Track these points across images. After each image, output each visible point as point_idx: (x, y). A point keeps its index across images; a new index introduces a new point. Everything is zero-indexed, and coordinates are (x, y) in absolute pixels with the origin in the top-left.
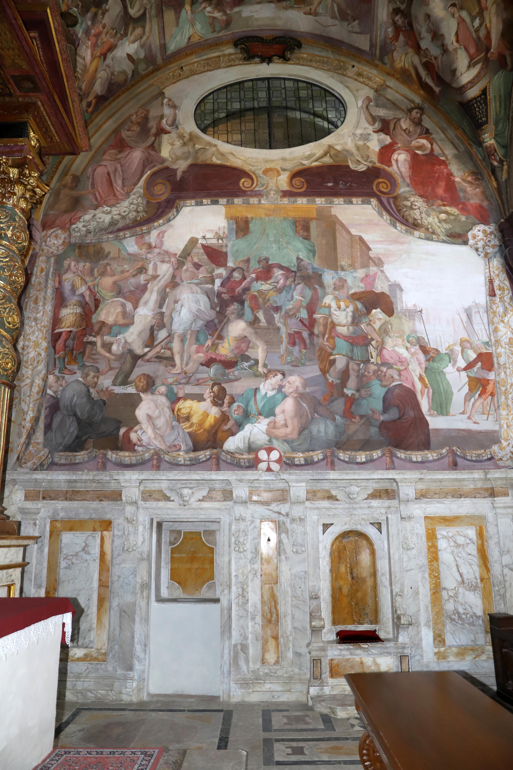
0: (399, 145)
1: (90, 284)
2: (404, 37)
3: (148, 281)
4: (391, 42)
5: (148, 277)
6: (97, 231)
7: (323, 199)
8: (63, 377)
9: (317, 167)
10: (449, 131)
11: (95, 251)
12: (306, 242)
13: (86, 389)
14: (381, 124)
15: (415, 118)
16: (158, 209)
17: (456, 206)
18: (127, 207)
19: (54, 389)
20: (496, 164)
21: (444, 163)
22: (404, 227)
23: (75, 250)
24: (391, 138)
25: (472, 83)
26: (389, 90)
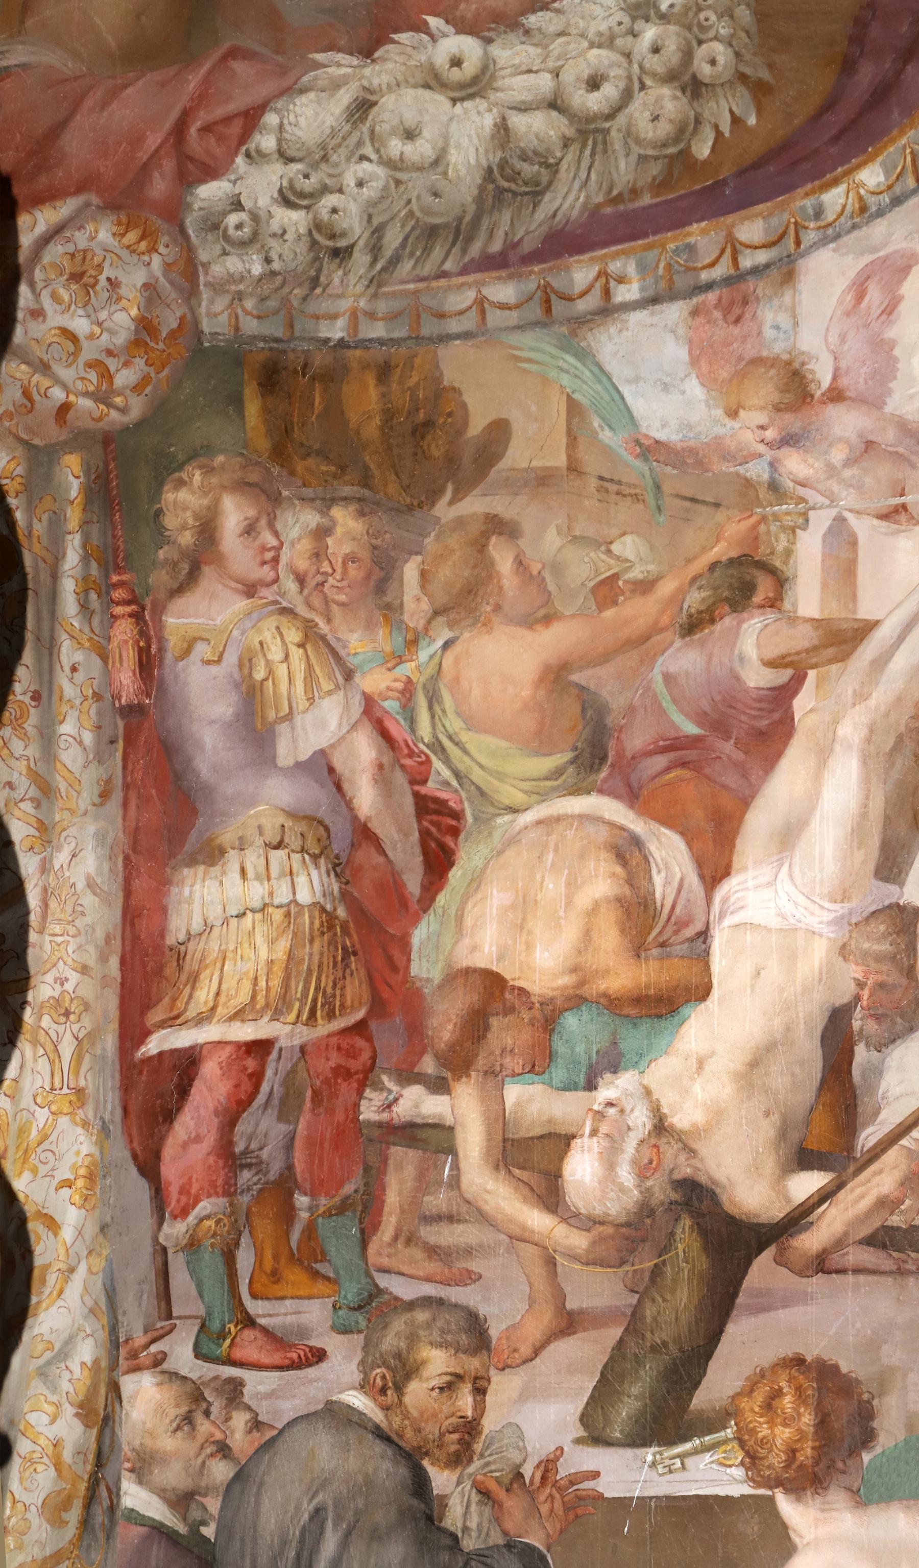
1: (375, 681)
3: (794, 671)
5: (801, 638)
6: (393, 239)
8: (234, 1389)
11: (389, 415)
13: (403, 1471)
16: (848, 66)
18: (607, 41)
19: (173, 1476)
23: (237, 402)
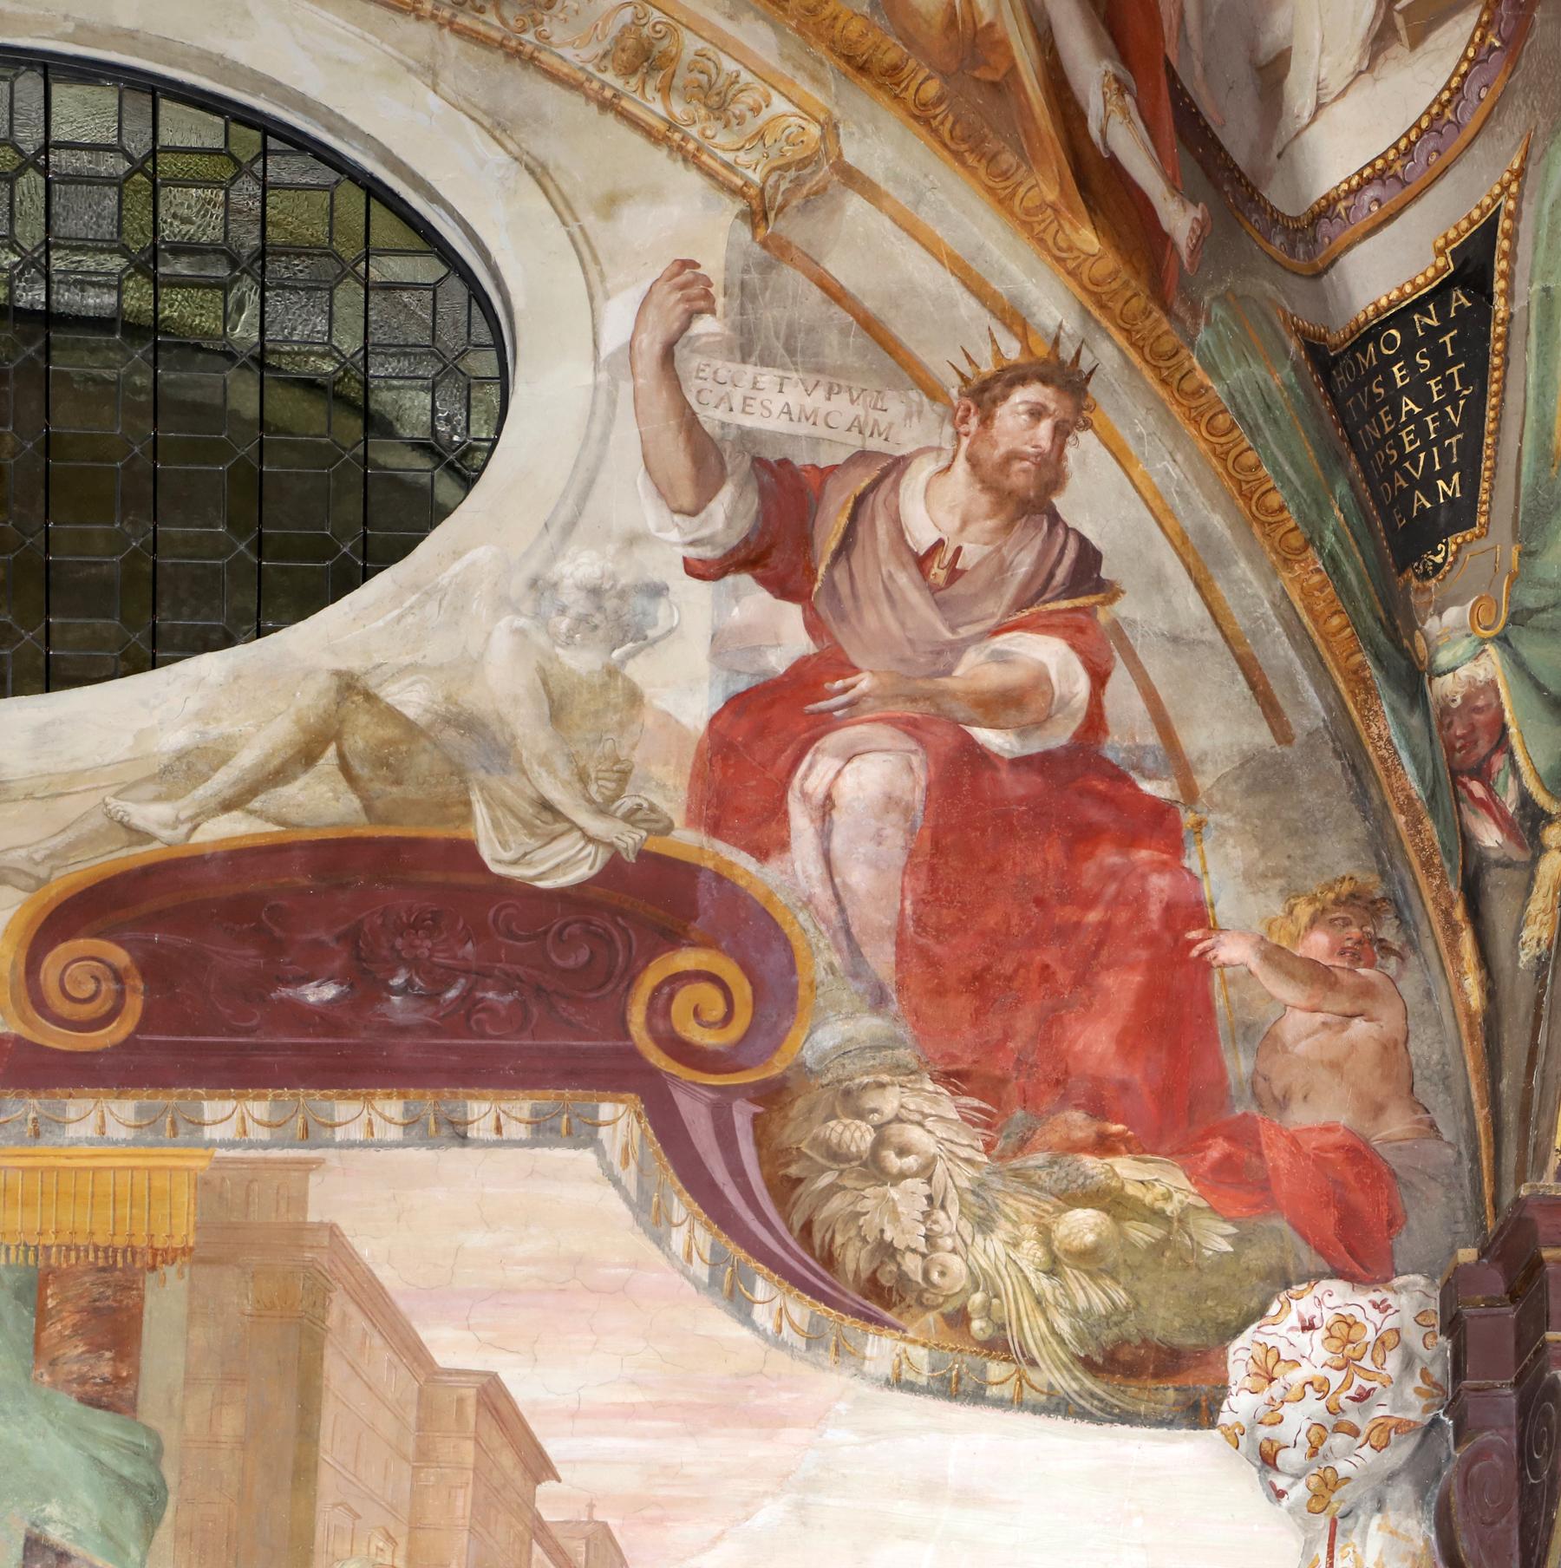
7: (258, 1108)
9: (240, 857)
10: (1243, 568)
12: (103, 1423)
14: (753, 502)
15: (1012, 456)
17: (1184, 1151)
21: (1160, 826)
22: (801, 1310)
24: (814, 626)
26: (855, 204)
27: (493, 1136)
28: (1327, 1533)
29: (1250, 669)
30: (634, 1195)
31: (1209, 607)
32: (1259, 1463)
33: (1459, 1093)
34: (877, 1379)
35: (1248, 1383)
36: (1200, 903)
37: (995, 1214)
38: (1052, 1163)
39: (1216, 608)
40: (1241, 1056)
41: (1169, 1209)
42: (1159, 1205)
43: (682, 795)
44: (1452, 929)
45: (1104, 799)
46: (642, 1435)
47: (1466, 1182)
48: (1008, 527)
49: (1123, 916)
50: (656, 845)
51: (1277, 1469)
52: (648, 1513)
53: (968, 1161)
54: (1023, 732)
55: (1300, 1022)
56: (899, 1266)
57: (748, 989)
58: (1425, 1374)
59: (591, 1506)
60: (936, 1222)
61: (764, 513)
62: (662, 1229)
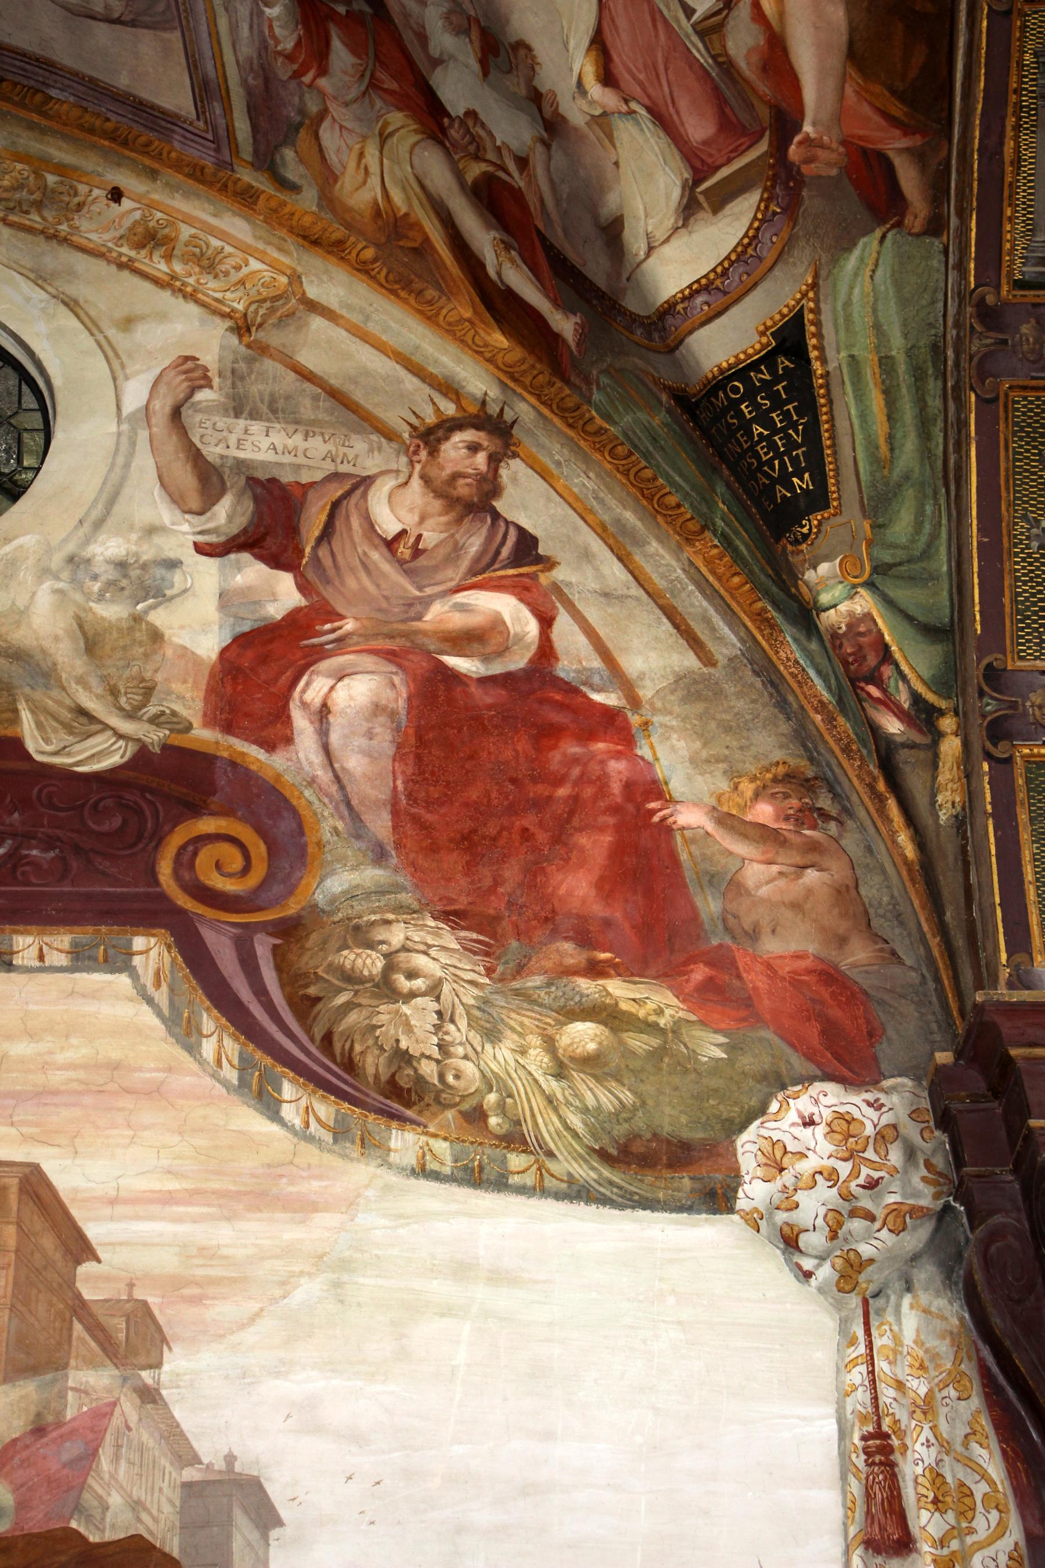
0: (349, 625)
2: (355, 52)
4: (297, 75)
10: (654, 546)
14: (249, 506)
15: (456, 476)
17: (670, 975)
20: (893, 726)
21: (612, 725)
22: (325, 1109)
24: (303, 587)
25: (717, 291)
26: (317, 323)
27: (37, 964)
28: (860, 1311)
29: (671, 614)
30: (166, 1011)
31: (631, 573)
32: (782, 1246)
33: (912, 925)
34: (403, 1169)
35: (759, 1172)
36: (655, 782)
37: (501, 1027)
38: (549, 984)
39: (637, 573)
40: (709, 898)
41: (662, 1022)
42: (653, 1018)
43: (199, 705)
44: (880, 799)
45: (562, 706)
46: (179, 1220)
47: (934, 999)
48: (459, 521)
49: (588, 792)
50: (177, 740)
51: (801, 1251)
52: (187, 1291)
53: (471, 982)
54: (486, 659)
55: (759, 873)
56: (416, 1070)
57: (263, 848)
58: (928, 1165)
59: (131, 1286)
60: (447, 1033)
61: (258, 513)
62: (193, 1039)
